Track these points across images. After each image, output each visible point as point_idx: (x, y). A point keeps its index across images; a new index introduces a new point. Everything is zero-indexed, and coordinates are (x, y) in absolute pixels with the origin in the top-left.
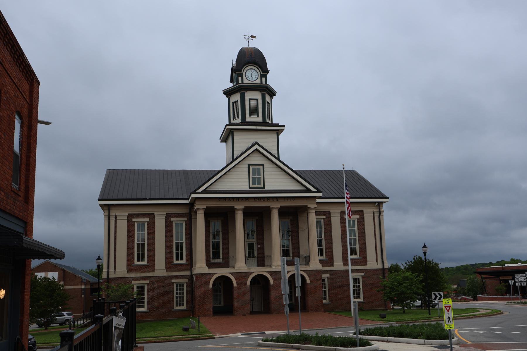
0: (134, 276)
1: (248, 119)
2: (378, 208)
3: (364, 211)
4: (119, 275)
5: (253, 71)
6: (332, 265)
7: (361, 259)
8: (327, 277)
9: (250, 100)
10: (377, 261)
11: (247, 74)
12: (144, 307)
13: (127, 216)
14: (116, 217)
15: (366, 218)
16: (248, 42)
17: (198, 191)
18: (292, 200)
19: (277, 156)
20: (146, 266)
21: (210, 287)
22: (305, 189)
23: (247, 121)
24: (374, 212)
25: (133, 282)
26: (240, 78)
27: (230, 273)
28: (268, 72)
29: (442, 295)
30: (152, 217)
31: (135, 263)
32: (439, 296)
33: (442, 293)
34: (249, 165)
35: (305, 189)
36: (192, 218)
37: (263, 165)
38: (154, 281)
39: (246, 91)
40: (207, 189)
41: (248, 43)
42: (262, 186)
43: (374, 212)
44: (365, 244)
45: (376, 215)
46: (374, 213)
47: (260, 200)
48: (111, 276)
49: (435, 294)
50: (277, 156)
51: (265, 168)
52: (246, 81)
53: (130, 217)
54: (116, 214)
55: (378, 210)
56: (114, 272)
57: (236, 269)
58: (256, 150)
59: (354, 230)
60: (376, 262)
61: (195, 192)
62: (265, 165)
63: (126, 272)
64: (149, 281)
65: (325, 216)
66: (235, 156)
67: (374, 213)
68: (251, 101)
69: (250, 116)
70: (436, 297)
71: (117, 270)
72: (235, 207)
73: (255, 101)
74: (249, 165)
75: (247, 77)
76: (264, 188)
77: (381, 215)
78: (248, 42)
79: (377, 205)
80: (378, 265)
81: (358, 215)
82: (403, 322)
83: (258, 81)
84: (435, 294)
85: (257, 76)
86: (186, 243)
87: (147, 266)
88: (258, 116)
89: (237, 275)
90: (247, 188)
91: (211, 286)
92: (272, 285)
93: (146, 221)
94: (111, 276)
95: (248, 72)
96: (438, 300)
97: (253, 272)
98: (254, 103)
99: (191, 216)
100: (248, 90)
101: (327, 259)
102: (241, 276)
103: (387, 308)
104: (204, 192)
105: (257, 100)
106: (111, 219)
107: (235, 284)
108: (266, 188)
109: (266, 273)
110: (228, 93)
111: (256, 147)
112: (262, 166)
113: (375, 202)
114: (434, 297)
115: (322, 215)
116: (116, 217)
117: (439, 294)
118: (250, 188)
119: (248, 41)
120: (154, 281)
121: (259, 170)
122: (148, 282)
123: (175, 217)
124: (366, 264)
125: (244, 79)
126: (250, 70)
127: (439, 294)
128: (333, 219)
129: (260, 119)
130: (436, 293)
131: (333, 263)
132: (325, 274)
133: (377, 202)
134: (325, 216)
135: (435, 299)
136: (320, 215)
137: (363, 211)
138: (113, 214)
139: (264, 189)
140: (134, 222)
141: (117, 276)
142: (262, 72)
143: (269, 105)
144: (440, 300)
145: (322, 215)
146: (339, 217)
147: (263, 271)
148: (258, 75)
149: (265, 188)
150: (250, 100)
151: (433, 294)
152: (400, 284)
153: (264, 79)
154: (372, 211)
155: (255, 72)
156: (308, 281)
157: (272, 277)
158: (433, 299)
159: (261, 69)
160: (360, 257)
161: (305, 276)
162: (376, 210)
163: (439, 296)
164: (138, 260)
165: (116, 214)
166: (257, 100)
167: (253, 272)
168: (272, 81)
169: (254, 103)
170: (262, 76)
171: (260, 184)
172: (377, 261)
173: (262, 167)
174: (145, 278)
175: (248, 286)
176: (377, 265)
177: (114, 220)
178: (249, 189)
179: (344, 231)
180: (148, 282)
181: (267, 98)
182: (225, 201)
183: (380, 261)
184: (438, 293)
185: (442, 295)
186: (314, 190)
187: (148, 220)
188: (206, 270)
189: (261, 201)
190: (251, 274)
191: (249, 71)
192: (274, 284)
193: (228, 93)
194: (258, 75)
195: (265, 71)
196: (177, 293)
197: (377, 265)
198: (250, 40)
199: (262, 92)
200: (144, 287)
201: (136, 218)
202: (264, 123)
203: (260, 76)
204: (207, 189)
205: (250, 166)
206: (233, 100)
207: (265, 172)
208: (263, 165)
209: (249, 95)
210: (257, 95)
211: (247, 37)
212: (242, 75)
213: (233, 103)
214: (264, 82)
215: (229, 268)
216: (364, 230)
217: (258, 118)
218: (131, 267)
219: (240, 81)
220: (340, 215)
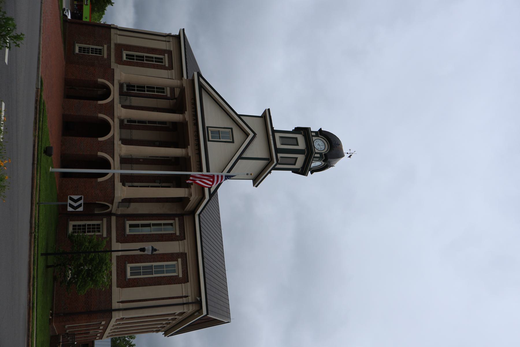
0: (112, 47)
1: (277, 135)
2: (193, 301)
3: (189, 284)
4: (113, 36)
5: (324, 147)
6: (118, 241)
7: (125, 280)
8: (103, 235)
9: (296, 138)
10: (122, 302)
11: (319, 141)
12: (79, 52)
13: (170, 49)
15: (179, 286)
16: (347, 153)
18: (197, 170)
19: (244, 156)
20: (122, 59)
21: (98, 79)
23: (275, 133)
24: (188, 296)
25: (105, 46)
27: (113, 99)
29: (77, 210)
31: (124, 52)
32: (75, 205)
34: (232, 129)
36: (171, 100)
37: (233, 142)
38: (106, 62)
39: (304, 135)
40: (202, 89)
42: (210, 139)
43: (188, 296)
44: (146, 285)
45: (185, 300)
46: (186, 297)
47: (196, 137)
48: (112, 30)
49: (80, 199)
50: (244, 156)
51: (230, 143)
53: (170, 53)
55: (190, 301)
56: (116, 33)
57: (117, 105)
58: (247, 135)
59: (163, 272)
60: (121, 300)
62: (233, 144)
63: (116, 42)
64: (106, 58)
65: (179, 235)
67: (186, 297)
68: (295, 140)
69: (281, 137)
70: (76, 201)
71: (118, 36)
73: (296, 143)
74: (232, 129)
75: (317, 140)
76: (209, 141)
77: (185, 306)
78: (347, 153)
79: (197, 300)
80: (117, 304)
81: (183, 276)
82: (38, 103)
84: (80, 199)
85: (319, 149)
87: (122, 60)
88: (282, 144)
89: (112, 104)
90: (207, 125)
91: (100, 80)
92: (98, 139)
93: (165, 64)
94: (112, 30)
95: (321, 142)
96: (69, 203)
97: (114, 121)
99: (172, 100)
100: (304, 137)
101: (126, 236)
102: (110, 109)
103: (54, 315)
104: (201, 86)
105: (297, 145)
106: (167, 37)
107: (100, 102)
108: (209, 143)
109: (113, 134)
111: (252, 135)
112: (231, 141)
113: (200, 296)
114: (76, 197)
115: (180, 231)
117: (80, 206)
118: (208, 127)
120: (106, 62)
122: (105, 56)
124: (118, 286)
125: (315, 137)
126: (323, 144)
127: (80, 206)
128: (176, 243)
130: (82, 202)
131: (120, 243)
132: (107, 232)
133: (201, 299)
134: (179, 235)
135: (71, 199)
136: (179, 229)
137: (188, 282)
138: (171, 39)
139: (208, 141)
140: (165, 55)
141: (112, 35)
142: (324, 154)
144: (70, 199)
145: (179, 232)
146: (178, 251)
147: (115, 131)
148: (321, 151)
149: (209, 142)
150: (296, 138)
151: (80, 196)
154: (189, 294)
155: (323, 148)
156: (100, 180)
157: (107, 139)
158: (70, 196)
159: (328, 152)
160: (128, 279)
161: (110, 122)
162: (190, 299)
164: (127, 55)
166: (297, 145)
167: (114, 121)
170: (321, 154)
171: (212, 137)
172: (122, 302)
174: (109, 55)
175: (98, 115)
176: (118, 302)
177: (165, 49)
178: (207, 127)
180: (105, 56)
181: (301, 159)
182: (192, 104)
183: (122, 306)
184: (81, 204)
185: (77, 210)
187: (167, 65)
188: (117, 78)
189: (195, 137)
190: (112, 119)
191: (323, 143)
192: (99, 141)
194: (321, 151)
197: (118, 302)
199: (306, 150)
200: (101, 54)
203: (322, 152)
204: (202, 89)
205: (230, 130)
207: (226, 143)
208: (233, 142)
209: (300, 138)
210: (302, 145)
215: (120, 95)
216: (164, 284)
217: (280, 144)
218: (120, 48)
220: (181, 251)
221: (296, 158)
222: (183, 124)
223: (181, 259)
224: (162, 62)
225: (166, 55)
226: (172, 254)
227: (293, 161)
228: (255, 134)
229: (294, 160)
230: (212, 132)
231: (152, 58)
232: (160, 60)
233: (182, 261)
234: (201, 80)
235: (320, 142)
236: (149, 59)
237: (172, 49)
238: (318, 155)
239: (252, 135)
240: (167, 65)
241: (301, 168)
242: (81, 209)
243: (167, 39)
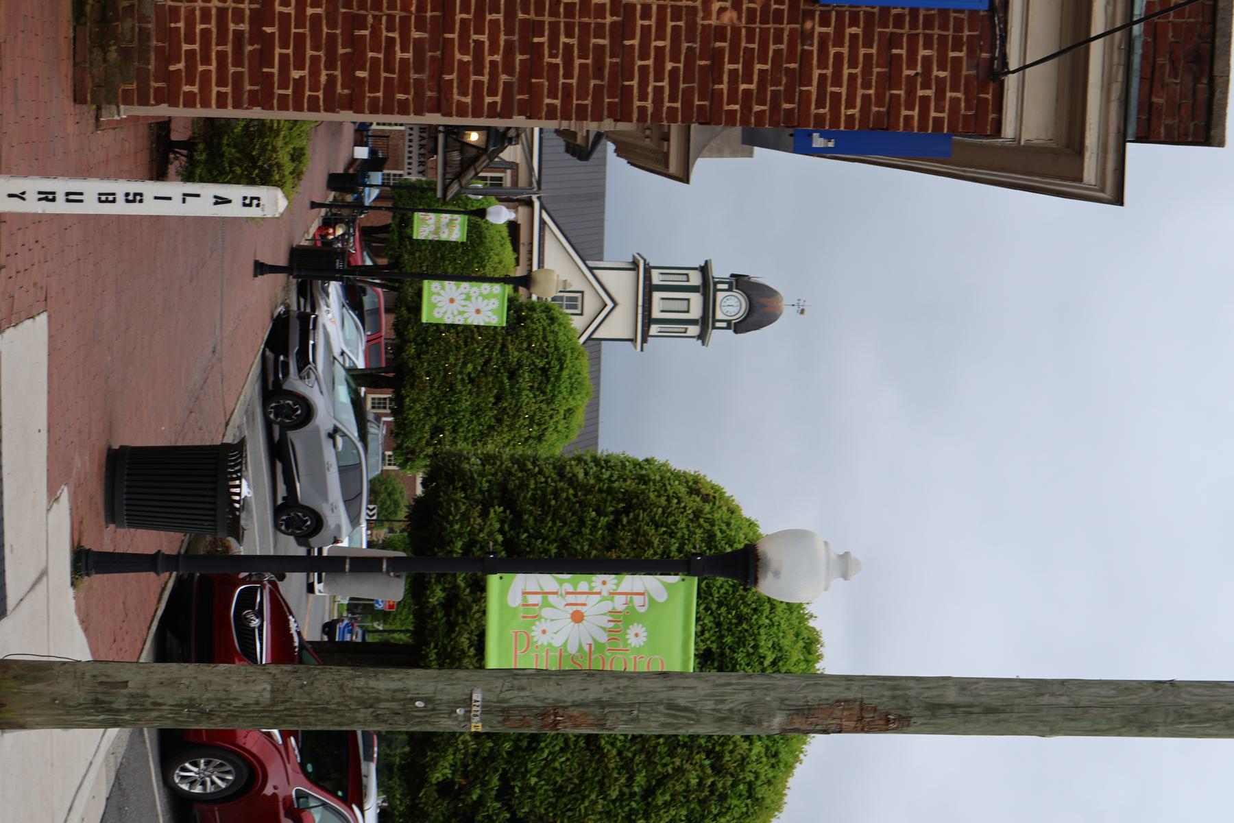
1: (657, 296)
26: (725, 286)
28: (736, 332)
33: (375, 518)
34: (582, 292)
52: (720, 295)
61: (542, 207)
66: (597, 272)
69: (663, 299)
83: (719, 316)
88: (662, 311)
98: (683, 306)
111: (610, 305)
121: (575, 307)
123: (512, 176)
129: (656, 314)
130: (375, 511)
143: (683, 335)
150: (688, 300)
152: (390, 495)
153: (724, 325)
163: (371, 513)
168: (720, 337)
169: (683, 306)
170: (729, 322)
173: (579, 312)
181: (694, 330)
193: (704, 270)
195: (740, 327)
196: (395, 175)
198: (796, 307)
202: (648, 320)
208: (581, 314)
209: (696, 299)
210: (696, 312)
211: (801, 303)
212: (730, 290)
214: (718, 324)
219: (720, 286)
228: (615, 304)
234: (545, 216)
235: (733, 301)
238: (724, 325)
242: (375, 518)
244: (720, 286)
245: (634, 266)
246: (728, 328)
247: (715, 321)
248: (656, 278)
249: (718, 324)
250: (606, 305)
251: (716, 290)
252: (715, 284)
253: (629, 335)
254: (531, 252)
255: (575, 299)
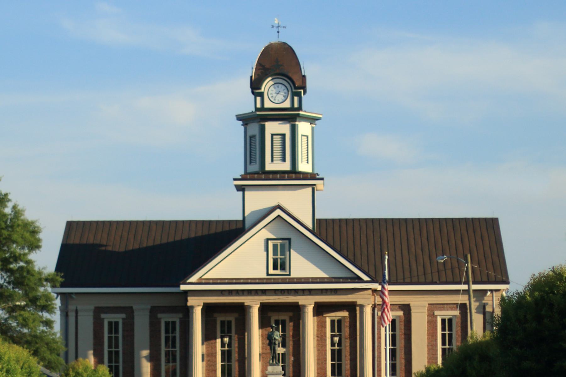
9: (273, 135)
14: (77, 312)
16: (278, 32)
17: (189, 281)
22: (356, 276)
30: (129, 311)
35: (356, 276)
41: (277, 33)
42: (288, 273)
53: (98, 311)
54: (77, 307)
69: (272, 161)
72: (246, 304)
75: (270, 96)
76: (289, 275)
78: (278, 32)
83: (287, 104)
86: (180, 352)
90: (264, 276)
105: (283, 136)
108: (293, 275)
110: (245, 119)
111: (278, 212)
116: (77, 312)
118: (268, 274)
119: (277, 30)
129: (286, 166)
133: (490, 290)
138: (72, 307)
150: (273, 135)
153: (296, 98)
165: (77, 307)
166: (283, 136)
169: (277, 139)
179: (432, 336)
186: (365, 278)
193: (245, 119)
201: (106, 313)
205: (270, 242)
206: (249, 133)
208: (289, 240)
209: (271, 127)
212: (261, 95)
213: (251, 137)
214: (296, 105)
221: (302, 135)
222: (265, 309)
223: (435, 310)
224: (117, 323)
225: (103, 316)
226: (429, 322)
227: (305, 139)
229: (303, 137)
230: (275, 268)
231: (110, 338)
232: (113, 326)
233: (437, 310)
236: (113, 342)
237: (92, 307)
238: (296, 98)
239: (278, 212)
240: (124, 316)
241: (311, 124)
243: (72, 316)
244: (259, 106)
245: (242, 189)
246: (299, 95)
247: (292, 108)
248: (255, 168)
249: (296, 105)
250: (279, 216)
251: (263, 109)
252: (257, 109)
253: (310, 189)
254: (230, 293)
255: (275, 246)
